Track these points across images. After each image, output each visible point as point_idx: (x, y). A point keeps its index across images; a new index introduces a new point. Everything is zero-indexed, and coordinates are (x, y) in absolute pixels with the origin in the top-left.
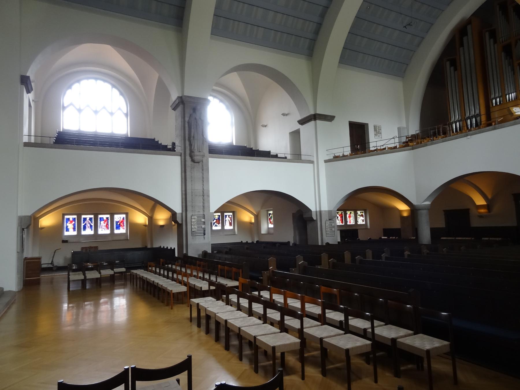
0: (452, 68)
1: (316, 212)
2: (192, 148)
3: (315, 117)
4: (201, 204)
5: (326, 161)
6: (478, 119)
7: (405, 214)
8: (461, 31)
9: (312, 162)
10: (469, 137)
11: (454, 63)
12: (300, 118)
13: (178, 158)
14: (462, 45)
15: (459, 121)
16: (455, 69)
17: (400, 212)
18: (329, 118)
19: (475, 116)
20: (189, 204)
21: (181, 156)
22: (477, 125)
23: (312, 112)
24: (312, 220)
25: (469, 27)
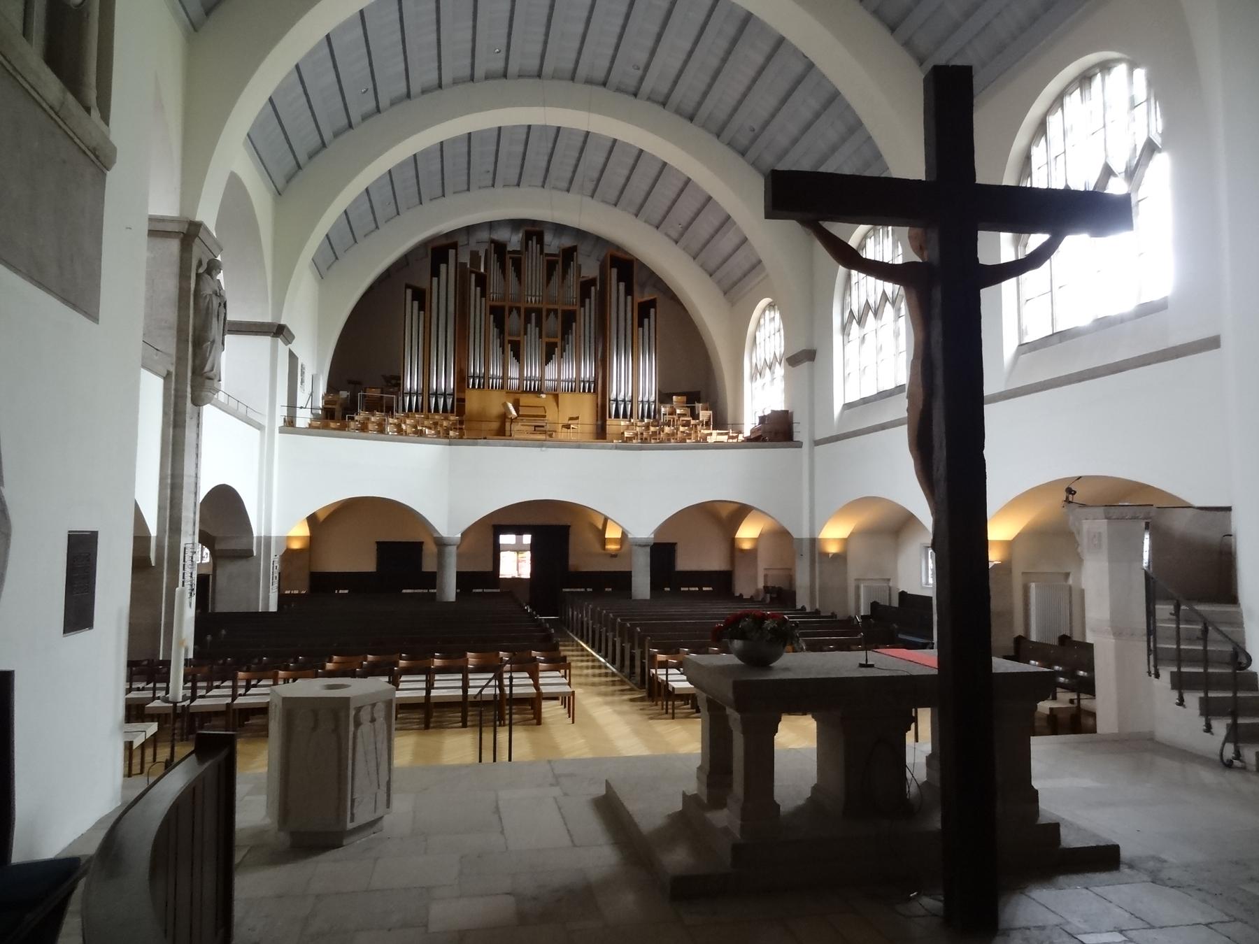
0: (416, 304)
2: (207, 368)
3: (279, 331)
6: (449, 401)
7: (296, 545)
8: (438, 251)
9: (260, 427)
11: (420, 296)
14: (435, 273)
15: (417, 394)
16: (422, 308)
19: (445, 395)
21: (167, 378)
22: (445, 410)
23: (268, 319)
24: (246, 554)
25: (452, 252)
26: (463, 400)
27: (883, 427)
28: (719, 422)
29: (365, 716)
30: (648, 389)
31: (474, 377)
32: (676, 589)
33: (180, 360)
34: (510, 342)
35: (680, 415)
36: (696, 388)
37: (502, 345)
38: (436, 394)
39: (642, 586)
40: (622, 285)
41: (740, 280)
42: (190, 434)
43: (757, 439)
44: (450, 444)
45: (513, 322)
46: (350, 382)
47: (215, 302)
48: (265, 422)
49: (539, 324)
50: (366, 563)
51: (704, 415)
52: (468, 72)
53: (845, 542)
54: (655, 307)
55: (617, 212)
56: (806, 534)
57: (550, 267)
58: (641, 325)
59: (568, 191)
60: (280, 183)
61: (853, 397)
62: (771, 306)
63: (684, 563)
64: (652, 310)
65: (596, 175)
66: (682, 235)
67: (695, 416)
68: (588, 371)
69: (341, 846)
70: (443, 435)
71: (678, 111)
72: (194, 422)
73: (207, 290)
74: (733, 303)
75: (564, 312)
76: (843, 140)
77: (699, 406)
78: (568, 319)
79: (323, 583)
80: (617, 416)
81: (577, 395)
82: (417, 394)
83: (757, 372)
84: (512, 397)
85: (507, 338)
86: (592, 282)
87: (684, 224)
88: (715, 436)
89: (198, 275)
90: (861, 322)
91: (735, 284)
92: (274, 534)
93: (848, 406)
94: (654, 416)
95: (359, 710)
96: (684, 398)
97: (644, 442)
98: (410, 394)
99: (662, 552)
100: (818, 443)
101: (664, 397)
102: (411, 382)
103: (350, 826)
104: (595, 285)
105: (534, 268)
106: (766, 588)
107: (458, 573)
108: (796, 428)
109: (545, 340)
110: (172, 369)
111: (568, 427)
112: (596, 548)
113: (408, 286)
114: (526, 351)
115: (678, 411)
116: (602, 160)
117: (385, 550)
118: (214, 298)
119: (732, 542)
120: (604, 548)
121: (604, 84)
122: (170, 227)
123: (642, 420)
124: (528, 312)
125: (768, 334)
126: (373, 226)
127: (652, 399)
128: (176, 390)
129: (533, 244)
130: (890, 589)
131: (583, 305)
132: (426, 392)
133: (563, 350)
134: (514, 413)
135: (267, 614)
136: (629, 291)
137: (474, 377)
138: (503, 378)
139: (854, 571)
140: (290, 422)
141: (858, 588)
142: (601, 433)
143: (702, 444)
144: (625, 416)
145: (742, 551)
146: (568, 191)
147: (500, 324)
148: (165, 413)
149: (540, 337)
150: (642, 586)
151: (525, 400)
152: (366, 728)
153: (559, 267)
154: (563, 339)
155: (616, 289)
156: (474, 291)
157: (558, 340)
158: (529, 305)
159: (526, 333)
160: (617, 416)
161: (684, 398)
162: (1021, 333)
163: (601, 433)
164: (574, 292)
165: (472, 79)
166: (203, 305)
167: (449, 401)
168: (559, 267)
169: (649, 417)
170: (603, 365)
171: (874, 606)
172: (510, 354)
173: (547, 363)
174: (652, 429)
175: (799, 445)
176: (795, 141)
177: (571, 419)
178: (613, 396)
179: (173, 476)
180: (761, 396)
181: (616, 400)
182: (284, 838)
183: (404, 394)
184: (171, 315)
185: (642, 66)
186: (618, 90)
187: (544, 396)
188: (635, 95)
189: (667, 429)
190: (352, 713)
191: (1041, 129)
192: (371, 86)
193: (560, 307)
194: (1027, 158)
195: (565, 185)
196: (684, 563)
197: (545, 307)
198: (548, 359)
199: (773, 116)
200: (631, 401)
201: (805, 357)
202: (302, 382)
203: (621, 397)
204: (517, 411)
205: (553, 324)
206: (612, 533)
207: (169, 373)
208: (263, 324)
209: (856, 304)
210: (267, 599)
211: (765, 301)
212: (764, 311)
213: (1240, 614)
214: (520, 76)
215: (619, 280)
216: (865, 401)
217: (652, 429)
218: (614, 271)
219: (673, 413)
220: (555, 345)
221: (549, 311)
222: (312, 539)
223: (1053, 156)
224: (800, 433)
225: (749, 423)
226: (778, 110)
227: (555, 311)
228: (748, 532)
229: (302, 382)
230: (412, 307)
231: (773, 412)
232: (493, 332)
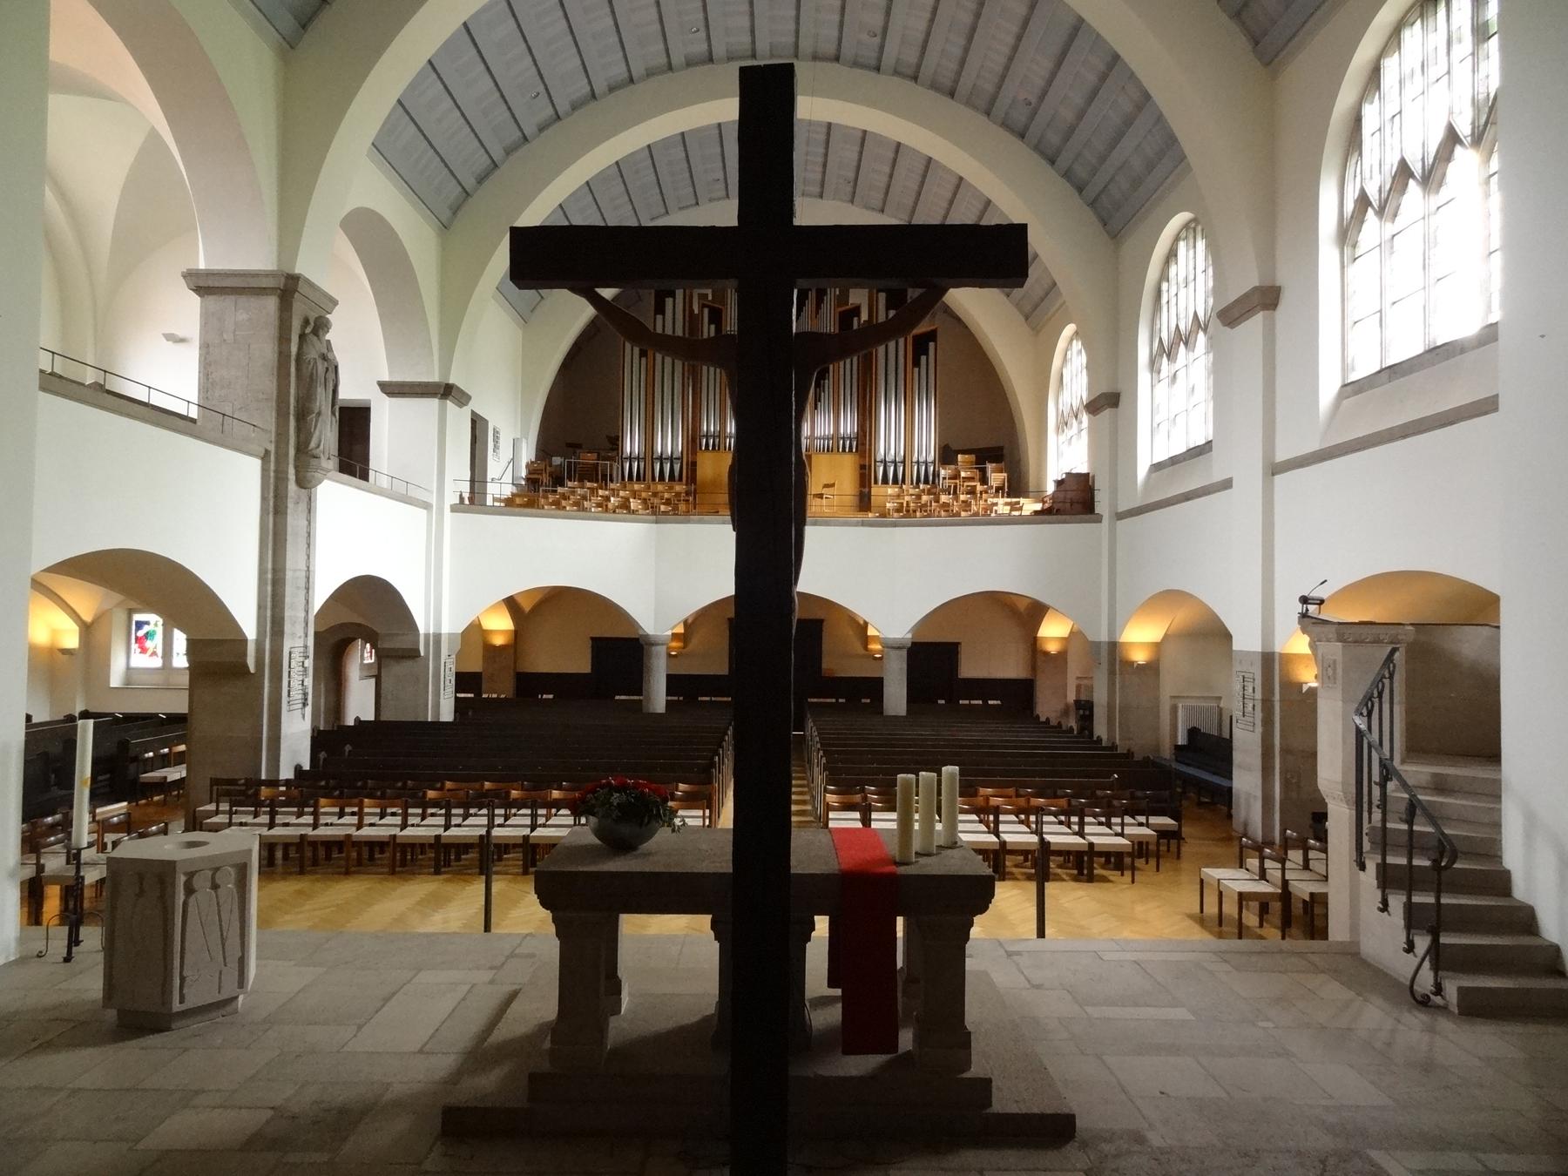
1: (427, 636)
2: (313, 445)
3: (446, 391)
4: (303, 614)
5: (454, 509)
6: (677, 467)
7: (499, 641)
9: (426, 506)
12: (386, 378)
13: (254, 465)
17: (485, 633)
18: (462, 398)
19: (671, 459)
20: (287, 614)
21: (265, 458)
23: (434, 377)
24: (413, 654)
26: (694, 464)
27: (1188, 497)
28: (1016, 487)
29: (202, 882)
30: (926, 445)
31: (707, 437)
32: (952, 700)
33: (281, 437)
36: (989, 444)
38: (661, 459)
39: (896, 698)
42: (294, 520)
43: (1051, 512)
46: (569, 445)
47: (321, 367)
48: (434, 501)
50: (579, 663)
51: (996, 478)
52: (663, 60)
53: (1157, 647)
56: (1104, 637)
58: (916, 363)
59: (821, 196)
60: (446, 215)
61: (1161, 456)
63: (970, 669)
64: (932, 345)
65: (851, 175)
67: (984, 481)
68: (848, 425)
69: (168, 1029)
70: (654, 511)
71: (934, 86)
72: (303, 506)
73: (312, 354)
74: (1036, 330)
77: (990, 467)
79: (529, 684)
80: (885, 481)
82: (638, 459)
83: (1063, 424)
88: (1002, 506)
89: (302, 337)
90: (1171, 354)
91: (1036, 307)
92: (445, 630)
93: (1157, 467)
94: (931, 480)
95: (191, 876)
96: (972, 457)
97: (907, 515)
98: (631, 459)
99: (931, 658)
100: (1121, 516)
101: (947, 455)
102: (632, 444)
103: (177, 1006)
104: (858, 315)
106: (1077, 702)
107: (669, 677)
108: (1098, 496)
110: (272, 448)
111: (820, 496)
112: (861, 651)
115: (963, 474)
116: (855, 156)
117: (601, 647)
118: (319, 362)
119: (1033, 643)
120: (866, 648)
121: (837, 59)
122: (265, 283)
125: (1073, 374)
127: (931, 458)
128: (276, 471)
130: (1221, 710)
132: (649, 455)
133: (817, 399)
135: (438, 725)
137: (707, 437)
139: (1168, 687)
140: (475, 499)
141: (1174, 709)
142: (864, 502)
143: (987, 519)
144: (895, 481)
145: (1046, 654)
146: (821, 196)
148: (264, 499)
150: (896, 698)
152: (203, 893)
160: (885, 481)
161: (972, 457)
162: (1345, 368)
163: (864, 502)
165: (670, 68)
166: (306, 372)
167: (677, 467)
169: (926, 482)
170: (866, 416)
171: (1193, 732)
174: (925, 498)
175: (1099, 519)
176: (1081, 115)
177: (826, 486)
179: (274, 570)
180: (1064, 453)
181: (885, 462)
182: (111, 1014)
184: (269, 385)
185: (879, 31)
188: (878, 69)
189: (944, 498)
190: (182, 879)
191: (1374, 78)
192: (541, 88)
194: (1357, 121)
195: (817, 190)
196: (970, 669)
199: (1050, 82)
200: (904, 462)
201: (1108, 402)
202: (496, 447)
203: (890, 457)
206: (871, 632)
207: (267, 452)
208: (427, 385)
209: (1167, 325)
210: (437, 705)
211: (1070, 329)
213: (1497, 783)
216: (1174, 461)
217: (925, 498)
219: (956, 476)
222: (517, 635)
223: (1388, 117)
224: (1102, 506)
226: (1053, 75)
228: (1053, 631)
229: (496, 447)
231: (1068, 474)
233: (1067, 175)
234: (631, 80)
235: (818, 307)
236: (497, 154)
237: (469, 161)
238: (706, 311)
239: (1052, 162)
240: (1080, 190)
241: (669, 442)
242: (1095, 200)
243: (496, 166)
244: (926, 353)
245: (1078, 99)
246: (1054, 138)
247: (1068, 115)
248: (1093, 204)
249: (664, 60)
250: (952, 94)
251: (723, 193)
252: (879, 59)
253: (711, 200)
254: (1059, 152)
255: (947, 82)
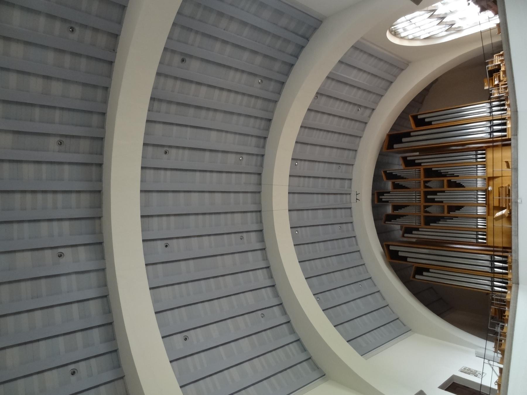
0: (425, 273)
10: (519, 201)
11: (420, 270)
14: (405, 259)
15: (492, 281)
16: (427, 270)
22: (505, 262)
25: (392, 248)
34: (449, 213)
35: (500, 81)
37: (451, 218)
40: (404, 140)
41: (386, 62)
44: (518, 284)
45: (434, 210)
49: (435, 193)
51: (497, 60)
54: (417, 116)
55: (360, 150)
57: (396, 186)
58: (430, 123)
62: (395, 34)
64: (419, 117)
65: (334, 166)
66: (366, 108)
67: (498, 69)
75: (425, 177)
76: (231, 18)
78: (430, 173)
80: (504, 130)
81: (489, 163)
82: (492, 281)
84: (491, 211)
85: (446, 214)
86: (404, 159)
87: (356, 108)
91: (391, 65)
101: (487, 97)
105: (398, 197)
109: (446, 188)
113: (414, 277)
114: (455, 202)
115: (496, 83)
116: (322, 165)
121: (260, 174)
123: (506, 110)
124: (427, 200)
126: (377, 294)
129: (384, 198)
131: (419, 164)
133: (453, 175)
134: (504, 211)
136: (408, 135)
138: (477, 218)
144: (505, 124)
147: (436, 219)
149: (444, 192)
151: (495, 201)
153: (397, 181)
154: (445, 176)
155: (407, 143)
156: (416, 235)
157: (445, 179)
158: (422, 200)
159: (442, 202)
160: (504, 130)
164: (412, 171)
168: (397, 181)
170: (465, 147)
172: (457, 213)
173: (463, 187)
178: (487, 136)
181: (490, 133)
183: (493, 291)
186: (262, 166)
187: (489, 189)
192: (260, 313)
193: (423, 179)
197: (422, 189)
198: (460, 185)
200: (490, 121)
204: (503, 209)
205: (434, 183)
211: (390, 38)
212: (402, 38)
214: (261, 222)
215: (401, 142)
218: (396, 146)
220: (449, 181)
221: (426, 187)
225: (489, 20)
227: (425, 182)
230: (426, 277)
232: (441, 224)
233: (296, 56)
234: (268, 267)
235: (403, 178)
236: (292, 338)
237: (293, 353)
238: (406, 235)
239: (292, 65)
240: (302, 47)
241: (483, 262)
242: (303, 36)
243: (298, 340)
244: (424, 118)
245: (246, 55)
246: (277, 66)
247: (259, 60)
248: (308, 39)
249: (259, 252)
250: (270, 120)
251: (350, 225)
252: (257, 155)
253: (353, 230)
254: (284, 63)
255: (263, 123)
